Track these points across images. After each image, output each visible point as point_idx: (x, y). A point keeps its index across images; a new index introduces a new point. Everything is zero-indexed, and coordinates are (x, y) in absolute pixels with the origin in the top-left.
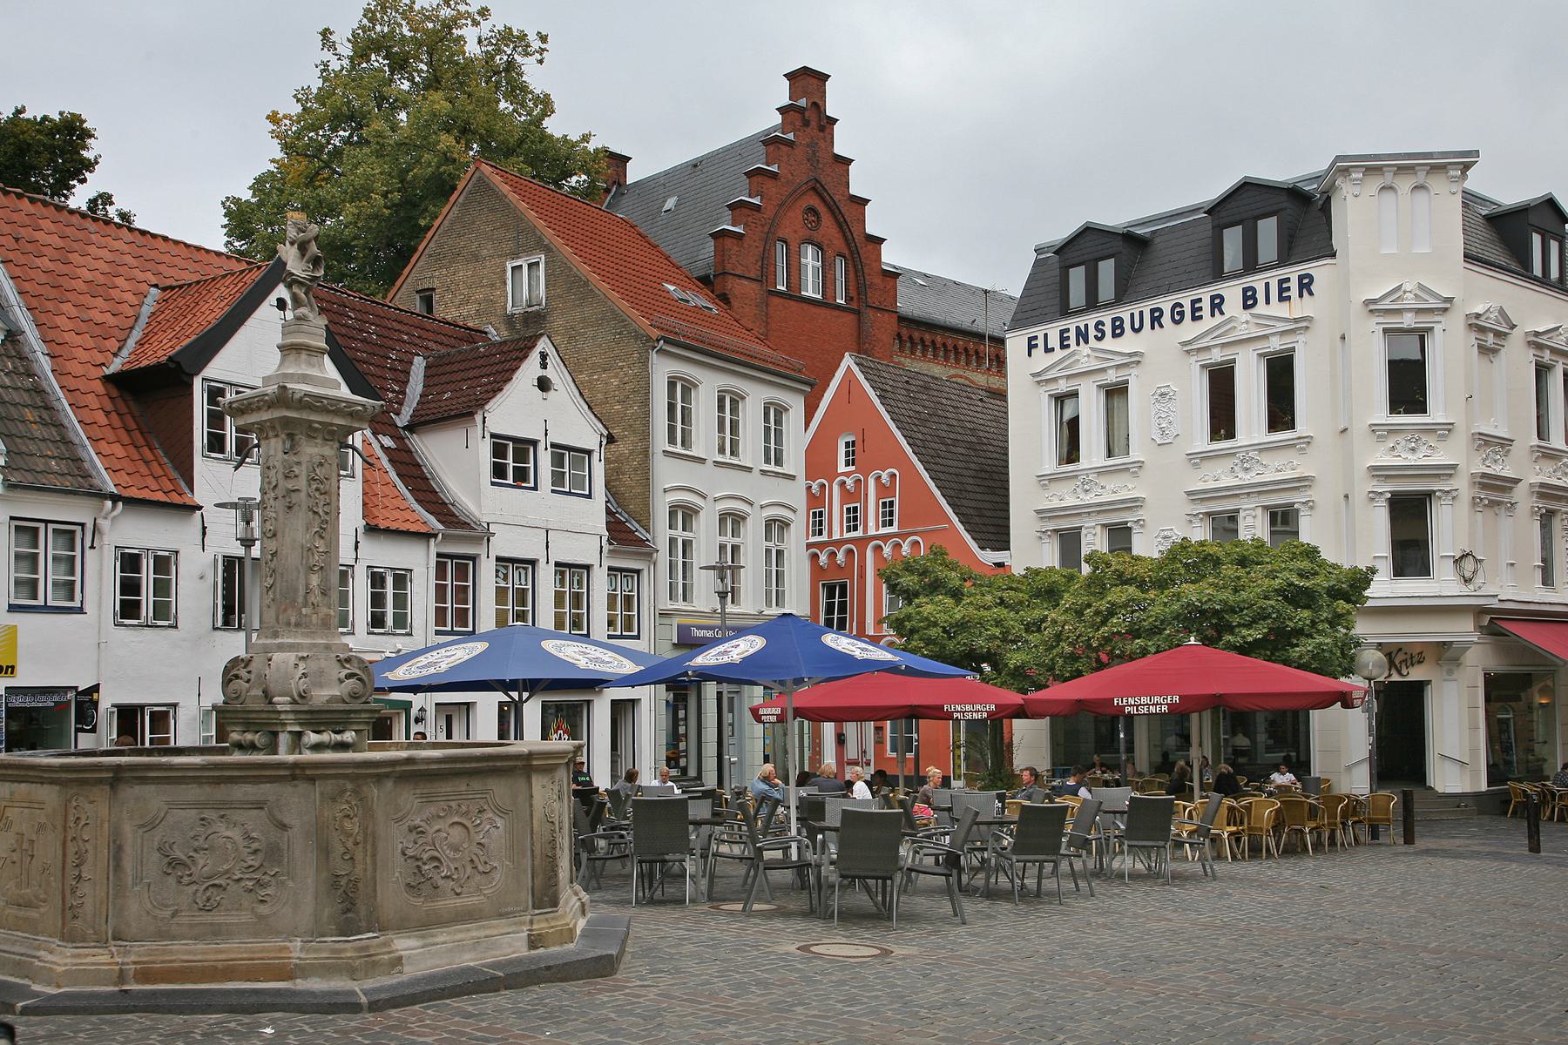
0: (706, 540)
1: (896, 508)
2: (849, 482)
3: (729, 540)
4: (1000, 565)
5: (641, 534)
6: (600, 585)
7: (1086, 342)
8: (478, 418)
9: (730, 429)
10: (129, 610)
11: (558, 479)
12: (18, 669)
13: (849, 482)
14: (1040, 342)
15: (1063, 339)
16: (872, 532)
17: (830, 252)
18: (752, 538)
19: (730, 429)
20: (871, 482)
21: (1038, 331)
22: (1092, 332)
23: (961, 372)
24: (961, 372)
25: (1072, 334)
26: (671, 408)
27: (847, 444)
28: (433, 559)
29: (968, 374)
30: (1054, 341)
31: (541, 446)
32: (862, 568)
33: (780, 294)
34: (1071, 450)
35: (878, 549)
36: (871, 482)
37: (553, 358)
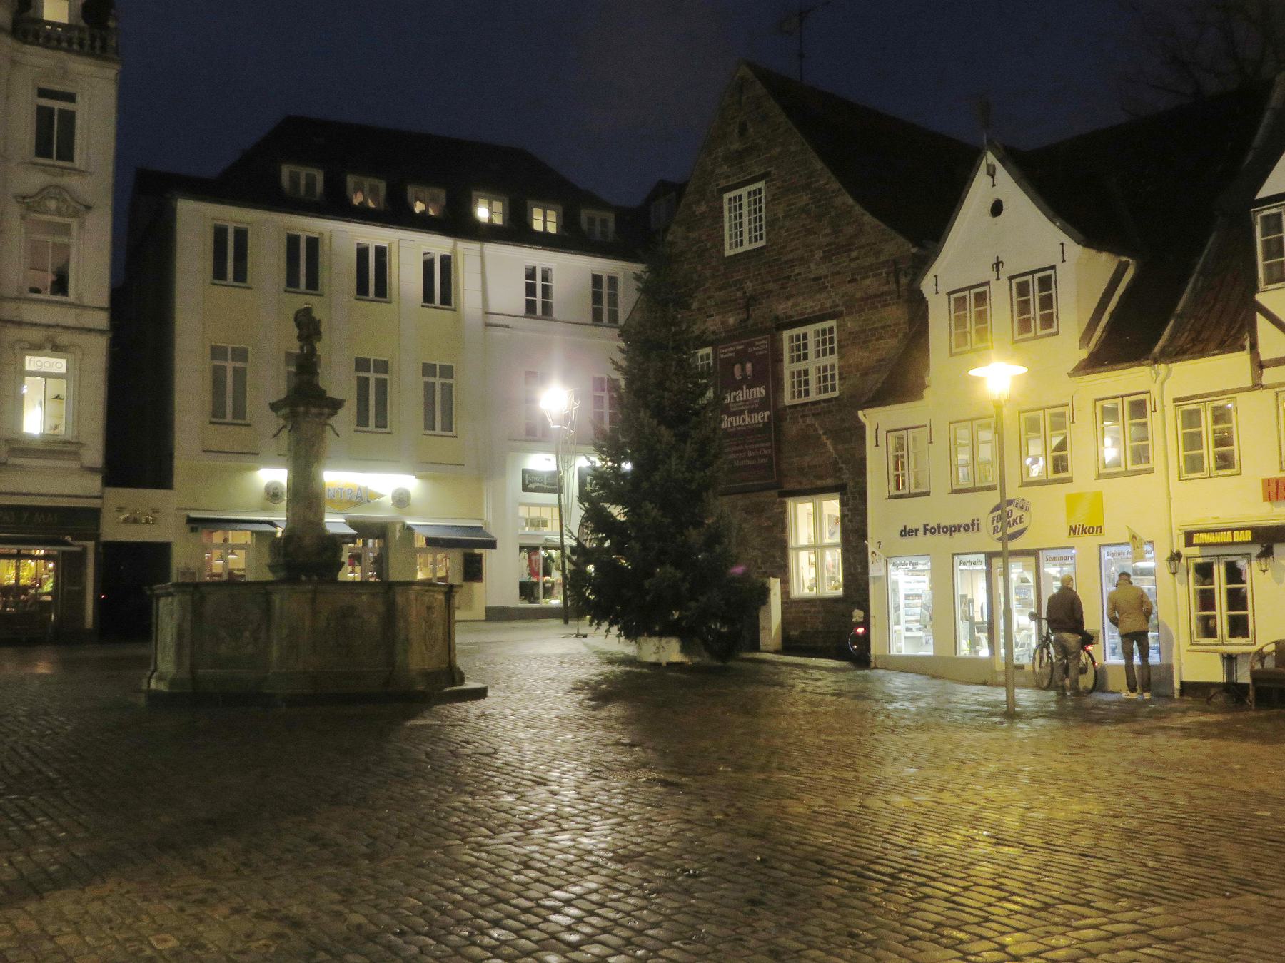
10: (1194, 465)
12: (1106, 529)
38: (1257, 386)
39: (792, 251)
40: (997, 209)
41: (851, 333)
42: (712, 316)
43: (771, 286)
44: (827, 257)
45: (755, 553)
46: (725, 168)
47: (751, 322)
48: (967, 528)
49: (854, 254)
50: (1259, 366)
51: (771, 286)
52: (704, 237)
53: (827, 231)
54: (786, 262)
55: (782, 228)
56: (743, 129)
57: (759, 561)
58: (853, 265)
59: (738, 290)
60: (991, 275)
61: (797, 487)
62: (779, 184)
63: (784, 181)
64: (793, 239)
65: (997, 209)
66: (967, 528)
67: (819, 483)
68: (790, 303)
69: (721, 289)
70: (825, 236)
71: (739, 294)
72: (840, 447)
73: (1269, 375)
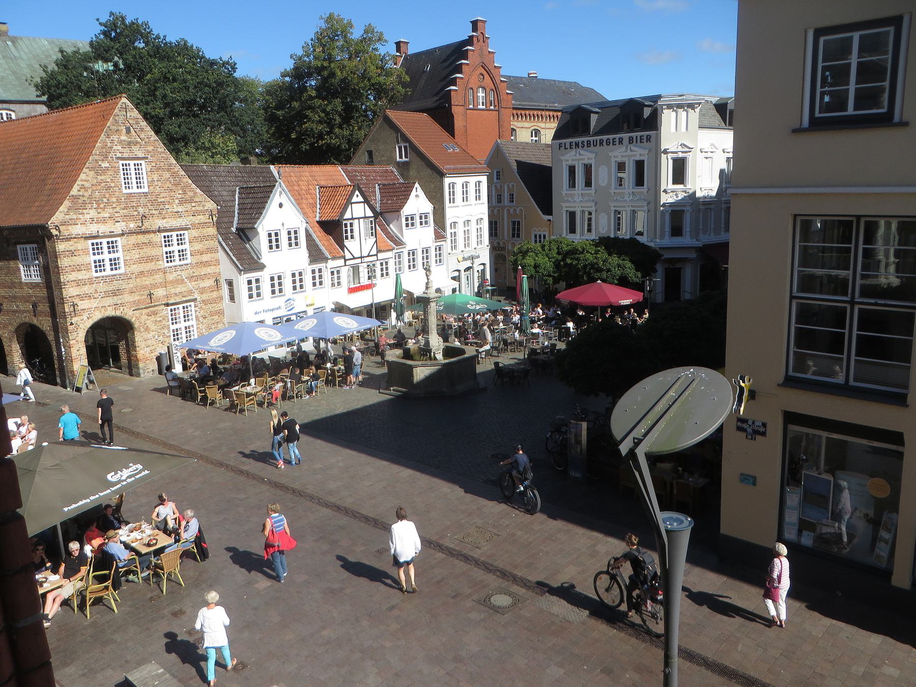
0: (460, 229)
1: (515, 196)
2: (498, 186)
3: (466, 229)
4: (550, 220)
5: (443, 233)
6: (432, 253)
7: (578, 147)
8: (401, 212)
9: (465, 193)
10: (333, 285)
11: (421, 223)
13: (498, 186)
14: (563, 145)
15: (571, 145)
16: (506, 204)
17: (488, 90)
18: (473, 227)
19: (465, 193)
20: (506, 186)
21: (563, 141)
22: (580, 145)
23: (535, 124)
24: (535, 124)
25: (574, 144)
26: (450, 192)
27: (497, 172)
28: (394, 254)
29: (538, 124)
30: (568, 146)
31: (417, 215)
32: (503, 216)
33: (471, 109)
34: (572, 184)
35: (508, 210)
36: (506, 186)
37: (419, 189)
38: (345, 265)
39: (163, 197)
40: (281, 205)
41: (195, 237)
42: (119, 222)
43: (154, 212)
44: (181, 203)
45: (154, 333)
46: (119, 148)
47: (143, 228)
48: (277, 309)
49: (193, 204)
50: (345, 261)
51: (154, 212)
52: (108, 180)
53: (180, 192)
54: (161, 202)
55: (157, 185)
56: (128, 131)
57: (156, 336)
58: (193, 209)
59: (135, 211)
60: (281, 228)
61: (174, 301)
62: (153, 164)
63: (156, 164)
64: (163, 192)
65: (281, 205)
66: (277, 309)
67: (184, 299)
68: (165, 221)
69: (124, 209)
70: (179, 194)
71: (135, 213)
72: (193, 283)
73: (348, 263)
